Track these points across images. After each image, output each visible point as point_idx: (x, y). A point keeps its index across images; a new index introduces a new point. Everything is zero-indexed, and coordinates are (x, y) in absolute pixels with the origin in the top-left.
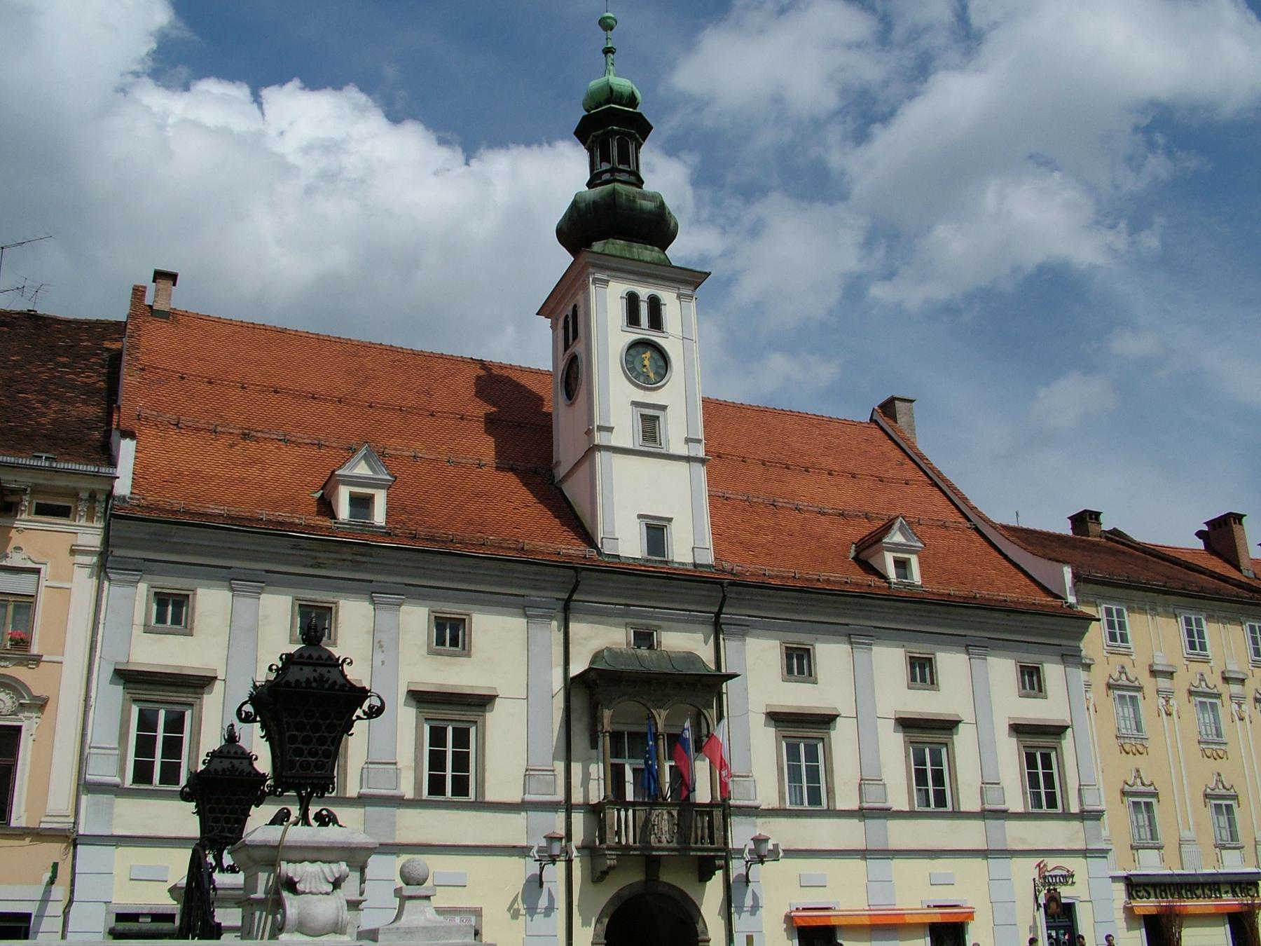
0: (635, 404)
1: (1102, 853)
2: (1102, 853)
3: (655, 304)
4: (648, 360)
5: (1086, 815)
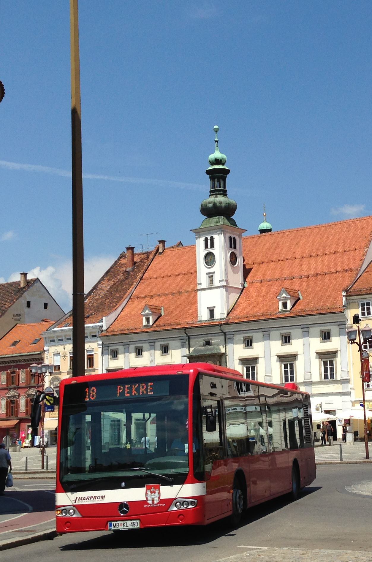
0: (207, 274)
1: (349, 394)
2: (349, 394)
3: (212, 239)
4: (210, 258)
5: (346, 381)
